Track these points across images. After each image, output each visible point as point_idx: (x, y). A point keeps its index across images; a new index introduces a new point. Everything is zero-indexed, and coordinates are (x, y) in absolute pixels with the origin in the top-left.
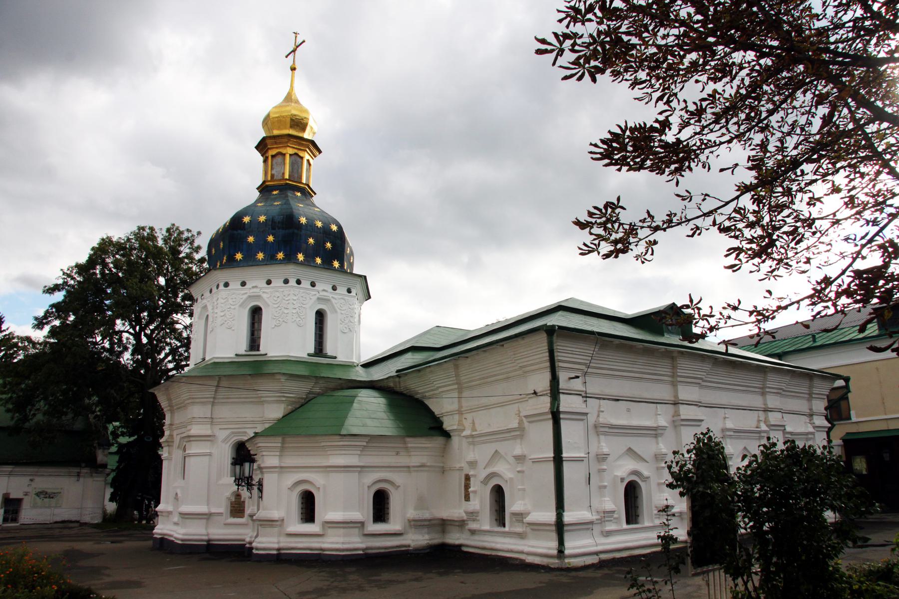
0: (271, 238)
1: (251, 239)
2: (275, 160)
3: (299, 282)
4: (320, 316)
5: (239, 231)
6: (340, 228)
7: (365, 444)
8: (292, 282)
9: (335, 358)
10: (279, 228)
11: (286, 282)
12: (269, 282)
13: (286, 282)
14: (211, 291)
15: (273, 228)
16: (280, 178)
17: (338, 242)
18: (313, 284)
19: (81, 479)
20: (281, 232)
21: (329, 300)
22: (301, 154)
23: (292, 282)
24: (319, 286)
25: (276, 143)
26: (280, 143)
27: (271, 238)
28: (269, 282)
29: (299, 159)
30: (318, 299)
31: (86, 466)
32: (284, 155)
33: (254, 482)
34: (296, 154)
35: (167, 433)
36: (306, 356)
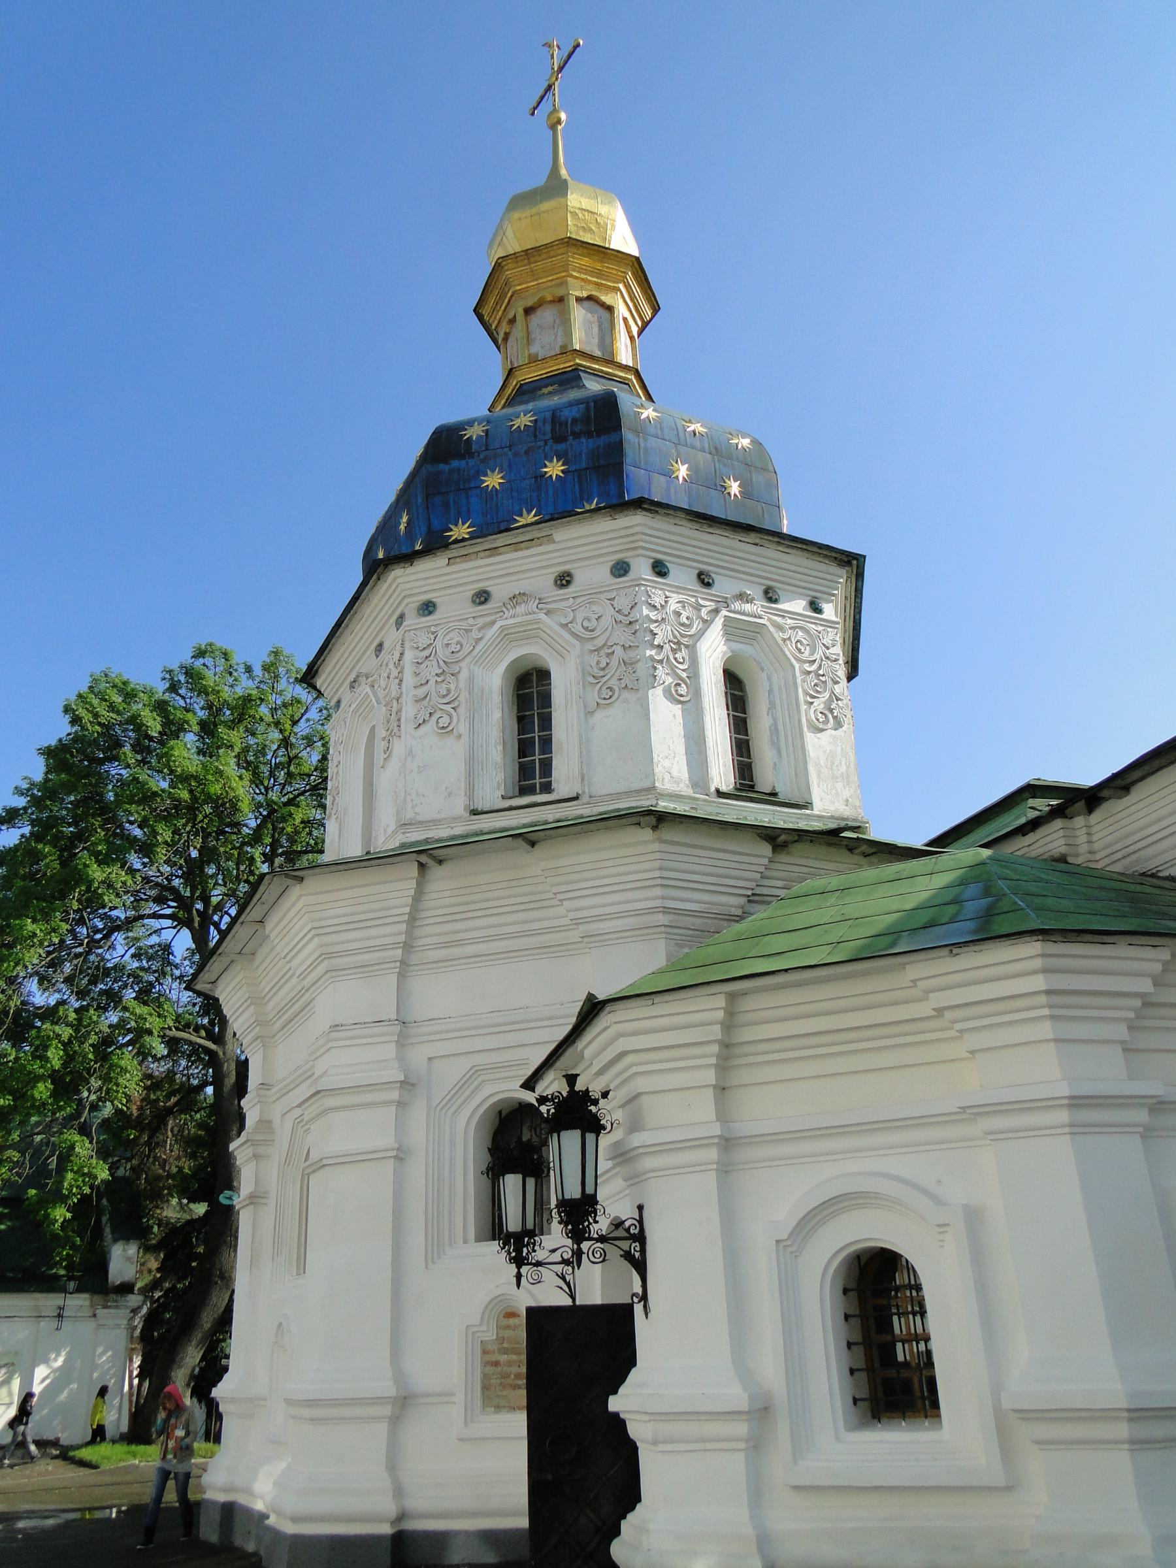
0: (554, 469)
1: (493, 480)
2: (535, 319)
3: (660, 569)
5: (455, 463)
7: (1146, 986)
8: (642, 569)
10: (576, 436)
11: (621, 569)
13: (621, 569)
15: (559, 439)
17: (758, 478)
19: (67, 1325)
20: (585, 445)
22: (607, 299)
23: (642, 569)
24: (724, 586)
28: (564, 580)
31: (79, 1290)
34: (590, 298)
35: (250, 1122)
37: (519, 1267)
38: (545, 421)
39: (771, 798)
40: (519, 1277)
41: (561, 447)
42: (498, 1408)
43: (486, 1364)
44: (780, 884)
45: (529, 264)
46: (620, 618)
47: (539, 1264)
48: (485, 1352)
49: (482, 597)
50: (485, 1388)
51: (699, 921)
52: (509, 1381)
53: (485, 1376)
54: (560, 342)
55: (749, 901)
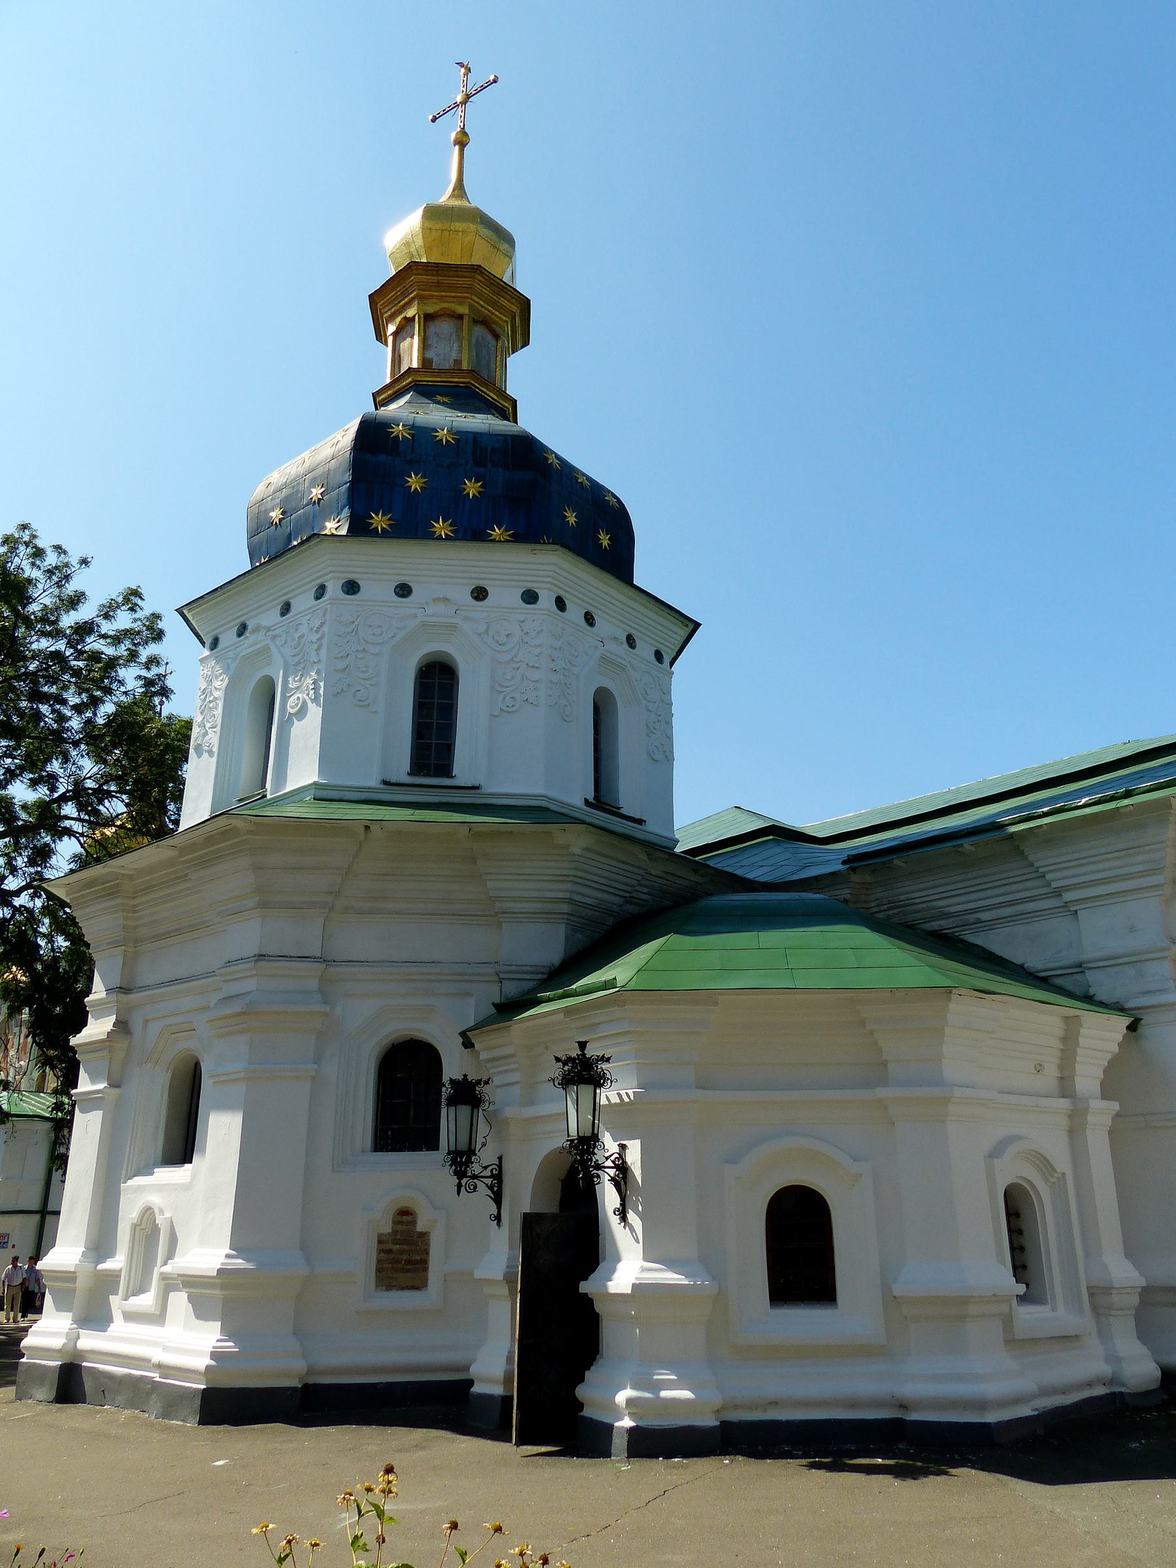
0: (472, 488)
2: (433, 328)
4: (602, 709)
5: (382, 458)
6: (619, 501)
9: (640, 822)
12: (480, 594)
13: (530, 597)
14: (321, 591)
16: (447, 365)
18: (589, 619)
21: (623, 668)
25: (438, 285)
26: (452, 287)
27: (472, 488)
29: (490, 338)
30: (604, 659)
32: (460, 317)
33: (476, 1168)
36: (580, 803)
37: (460, 1179)
38: (467, 442)
39: (615, 812)
40: (459, 1186)
41: (480, 470)
42: (389, 1288)
43: (380, 1251)
44: (646, 890)
45: (437, 275)
46: (526, 639)
47: (474, 1177)
48: (380, 1242)
49: (404, 590)
50: (378, 1271)
51: (590, 913)
52: (400, 1266)
53: (379, 1261)
54: (454, 356)
55: (627, 902)
